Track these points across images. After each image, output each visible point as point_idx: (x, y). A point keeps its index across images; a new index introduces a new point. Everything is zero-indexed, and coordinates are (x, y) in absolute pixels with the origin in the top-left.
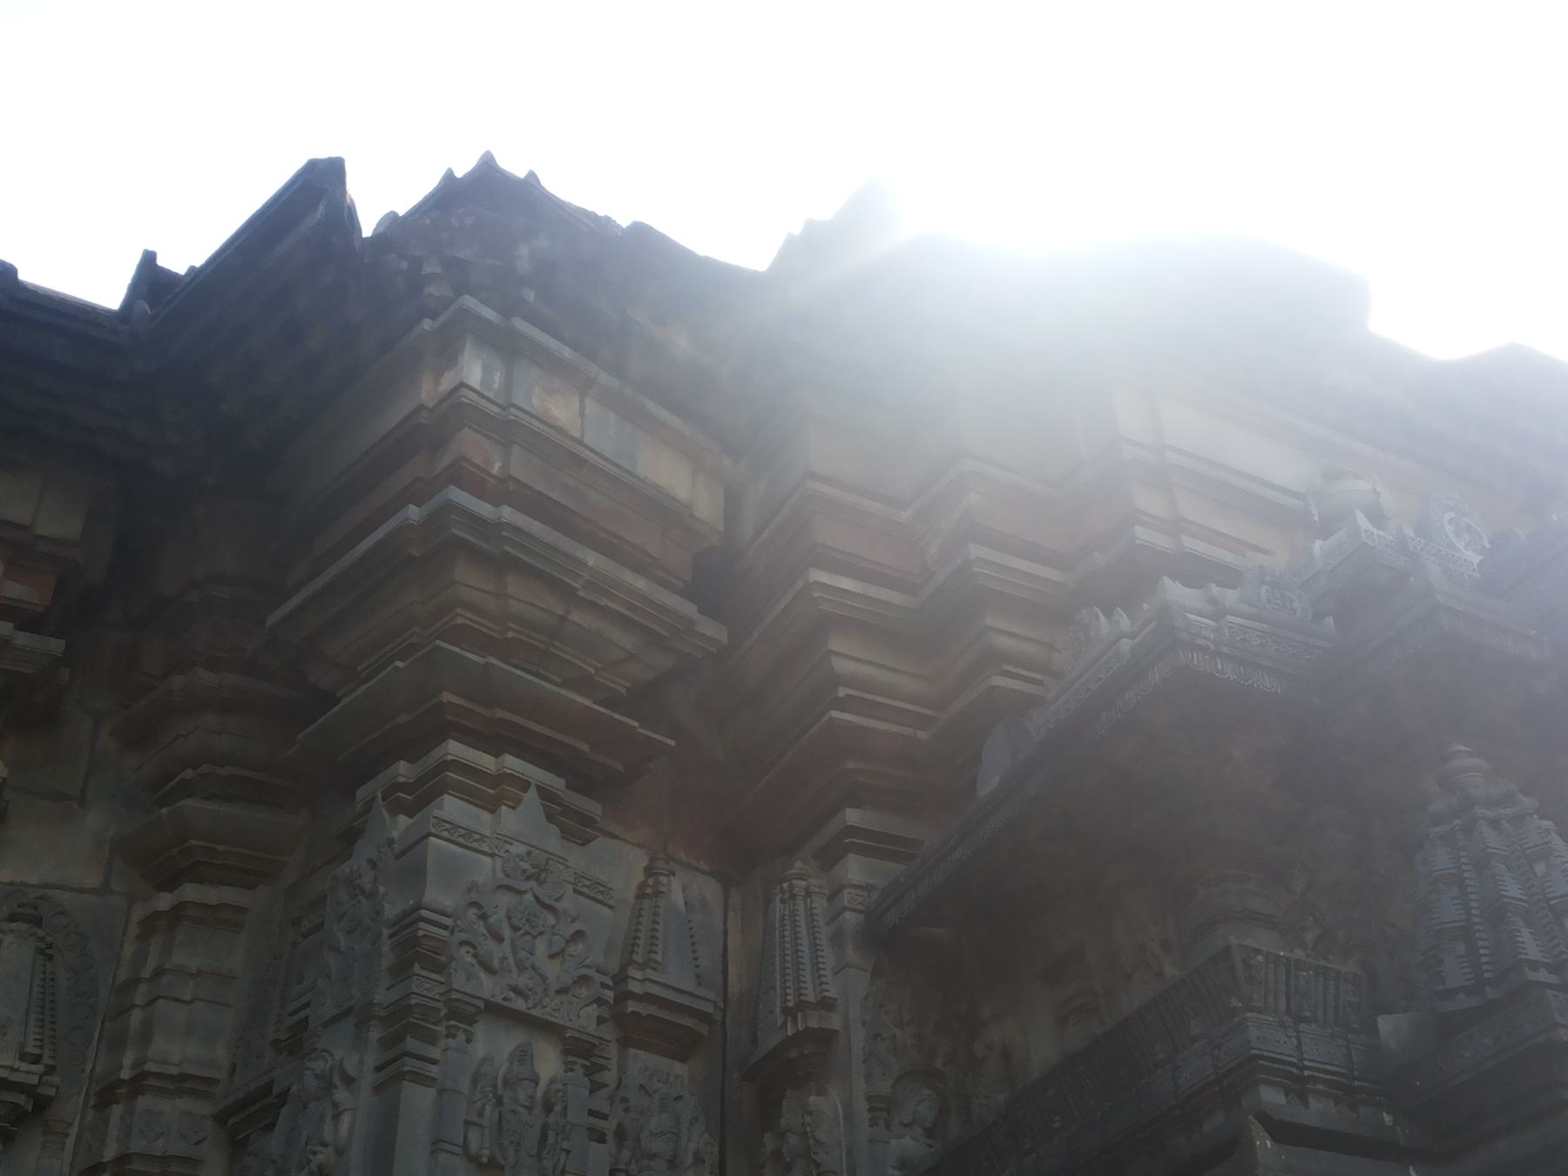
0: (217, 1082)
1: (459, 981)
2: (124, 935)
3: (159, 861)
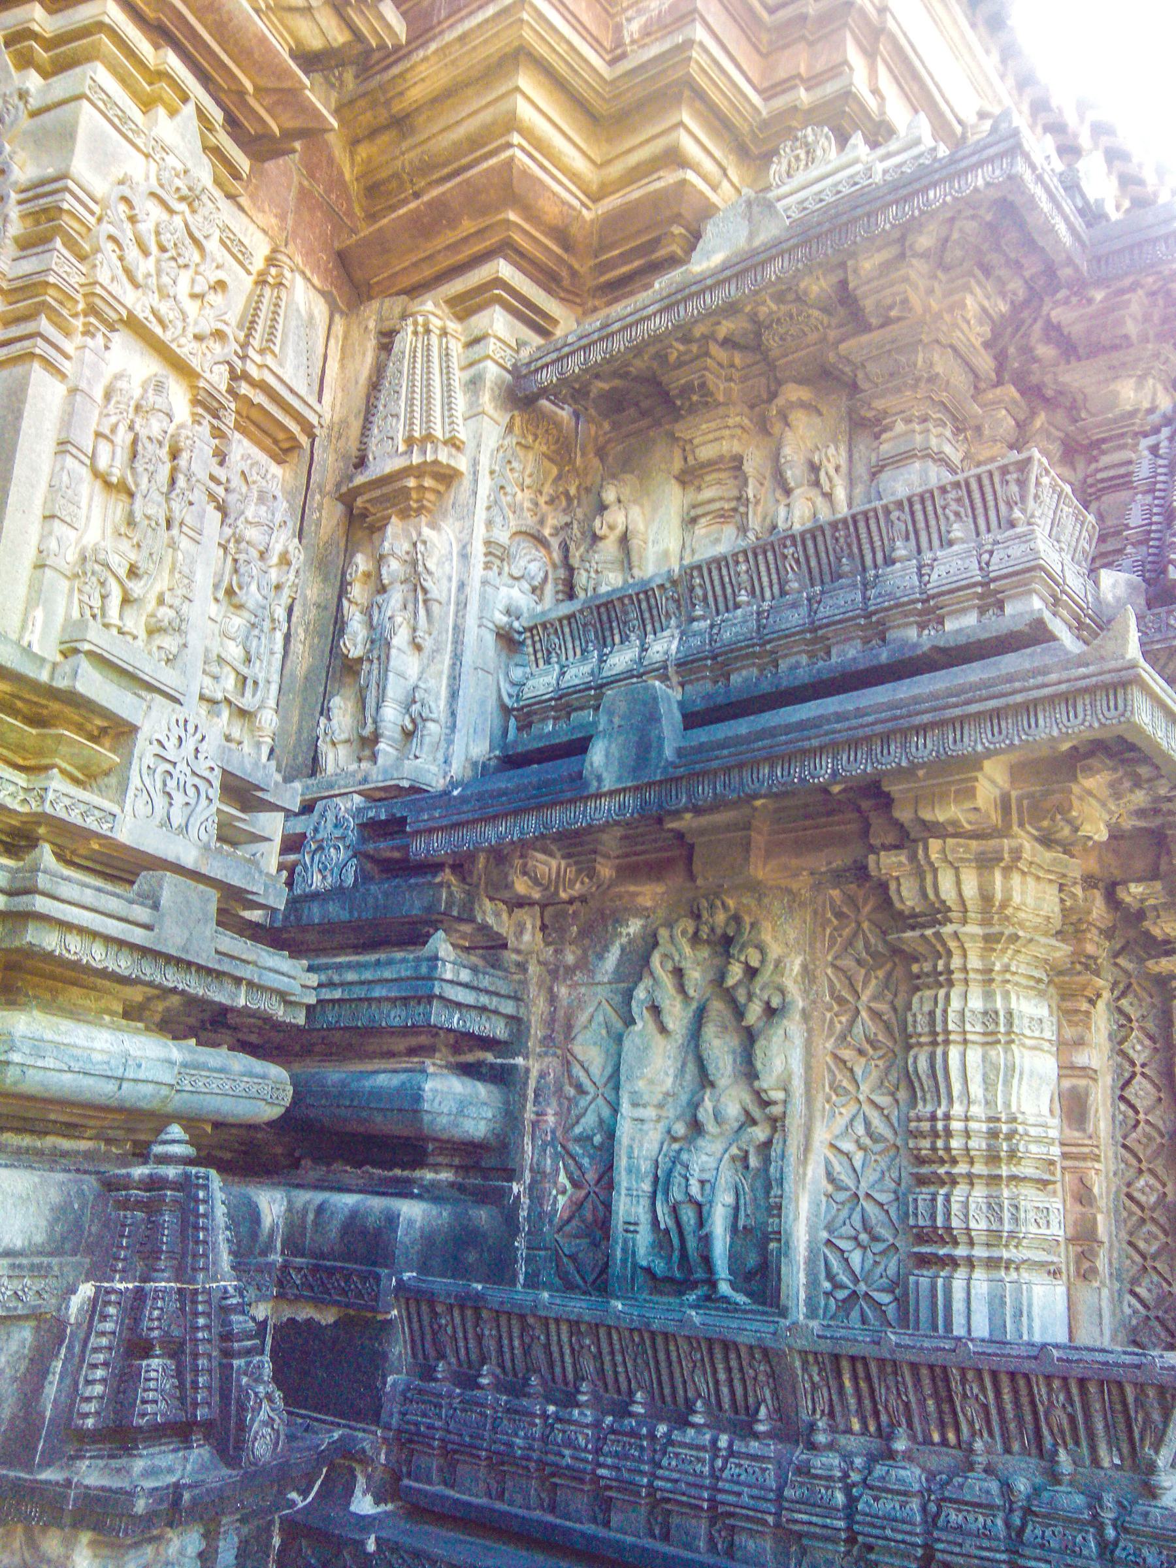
1: (103, 276)
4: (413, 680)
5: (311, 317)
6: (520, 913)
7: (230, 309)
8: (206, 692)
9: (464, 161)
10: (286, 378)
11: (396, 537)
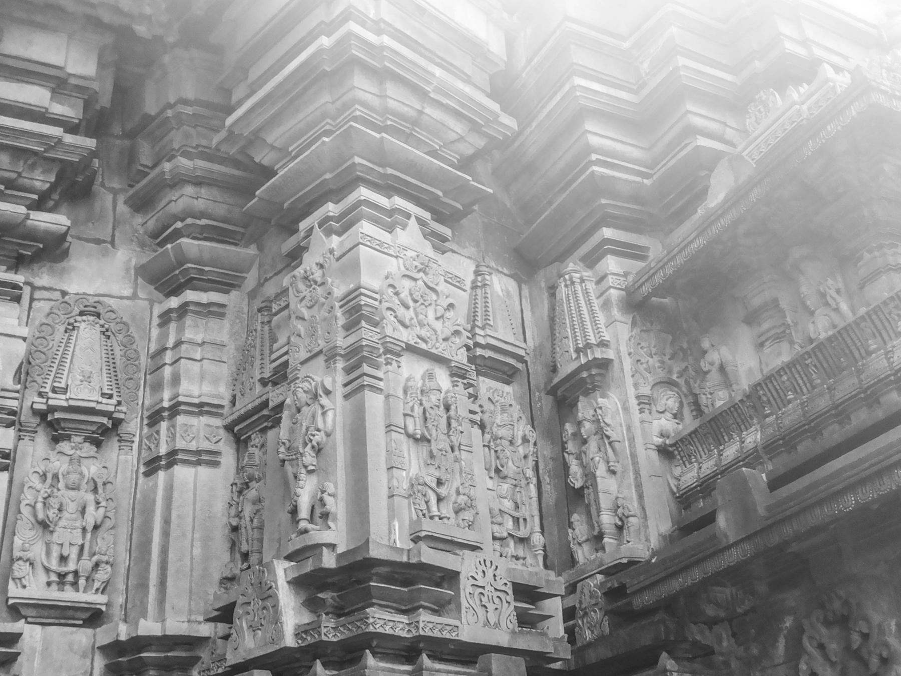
0: (222, 407)
1: (389, 331)
2: (150, 324)
3: (167, 279)
4: (615, 494)
5: (508, 293)
6: (716, 628)
7: (460, 317)
8: (497, 535)
9: (570, 177)
10: (500, 337)
11: (584, 410)
